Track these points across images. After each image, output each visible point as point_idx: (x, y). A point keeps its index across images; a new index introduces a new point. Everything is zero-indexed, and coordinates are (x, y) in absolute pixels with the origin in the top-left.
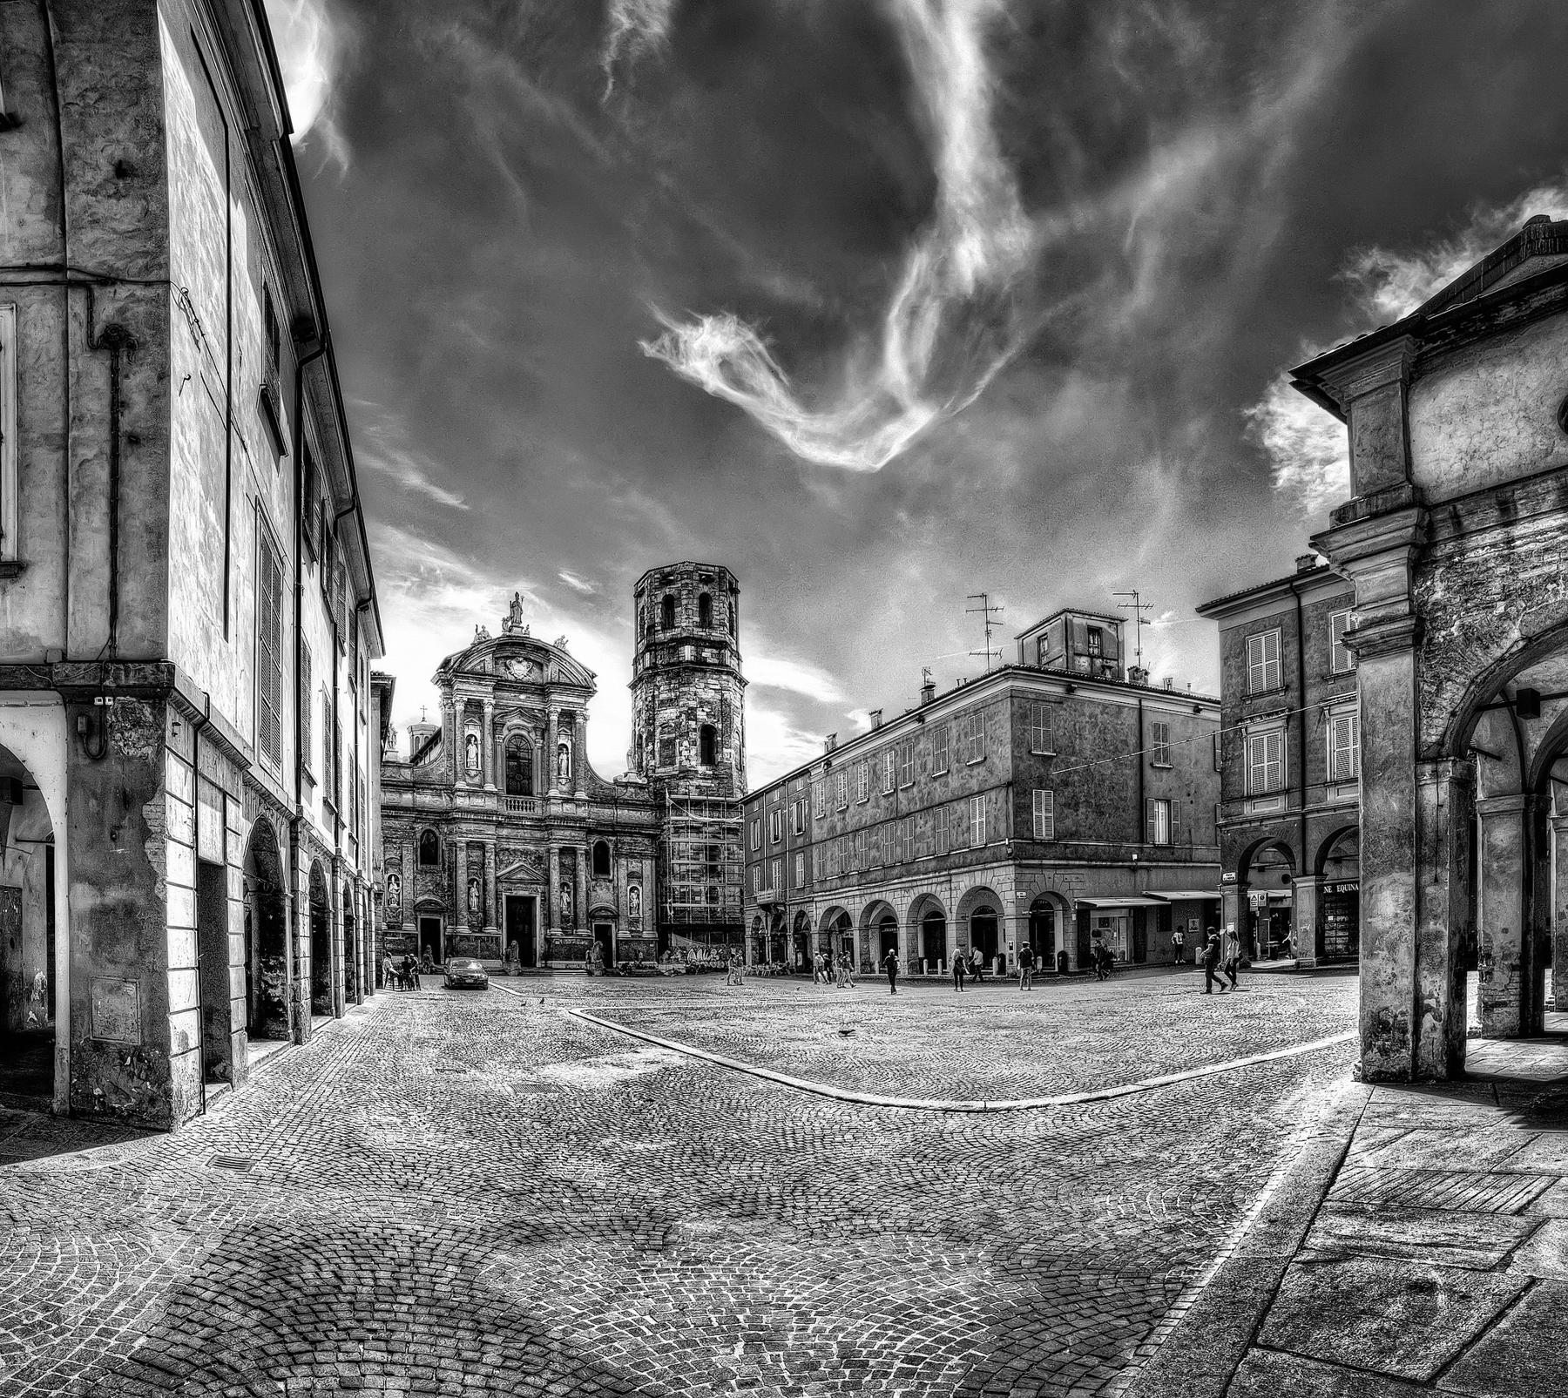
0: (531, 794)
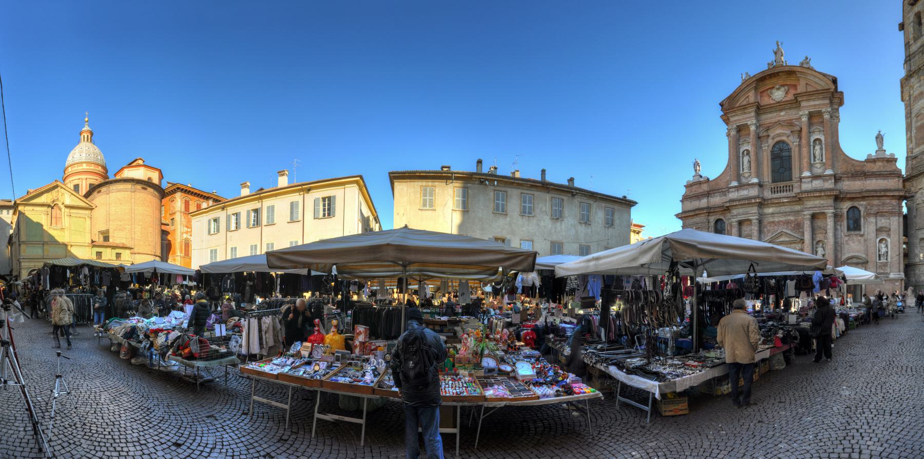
0: (791, 180)
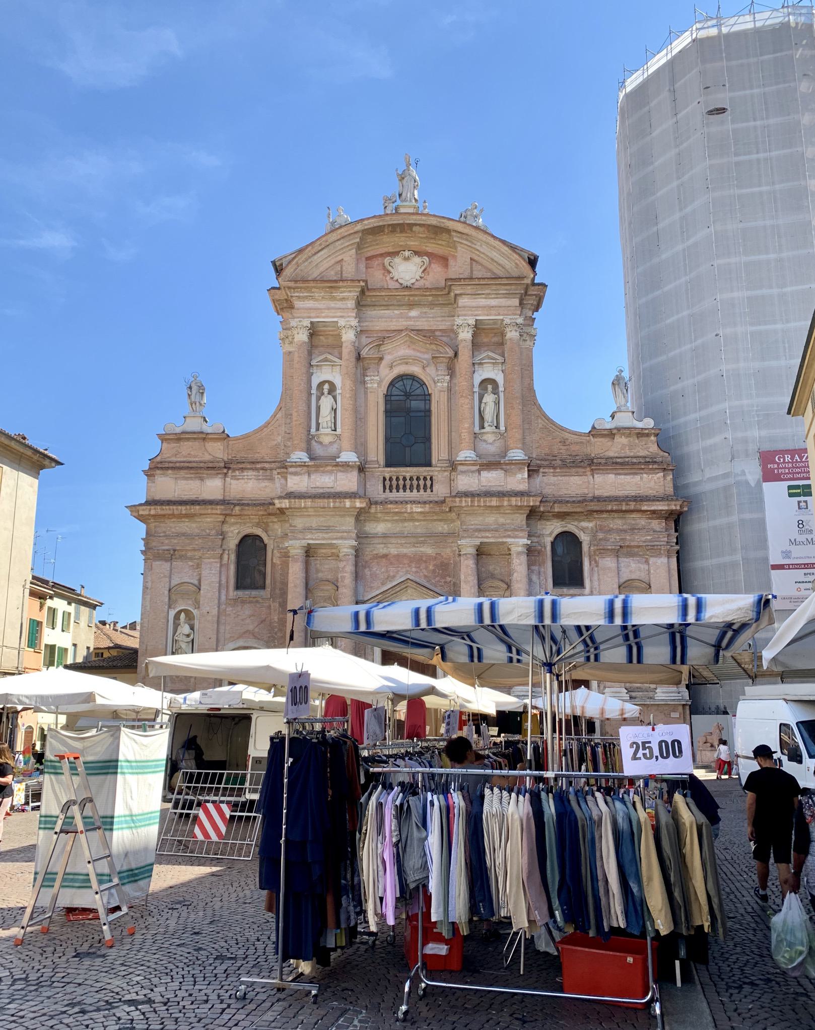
0: (429, 464)
